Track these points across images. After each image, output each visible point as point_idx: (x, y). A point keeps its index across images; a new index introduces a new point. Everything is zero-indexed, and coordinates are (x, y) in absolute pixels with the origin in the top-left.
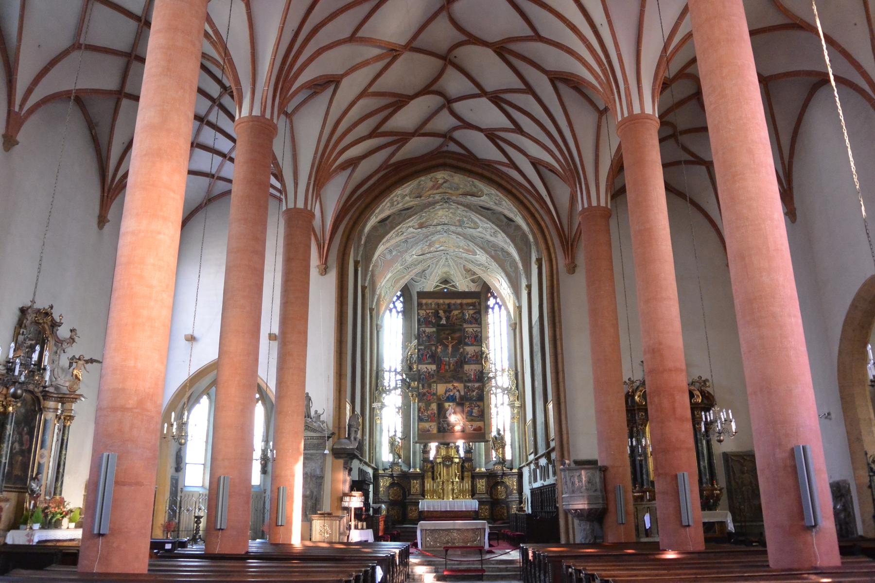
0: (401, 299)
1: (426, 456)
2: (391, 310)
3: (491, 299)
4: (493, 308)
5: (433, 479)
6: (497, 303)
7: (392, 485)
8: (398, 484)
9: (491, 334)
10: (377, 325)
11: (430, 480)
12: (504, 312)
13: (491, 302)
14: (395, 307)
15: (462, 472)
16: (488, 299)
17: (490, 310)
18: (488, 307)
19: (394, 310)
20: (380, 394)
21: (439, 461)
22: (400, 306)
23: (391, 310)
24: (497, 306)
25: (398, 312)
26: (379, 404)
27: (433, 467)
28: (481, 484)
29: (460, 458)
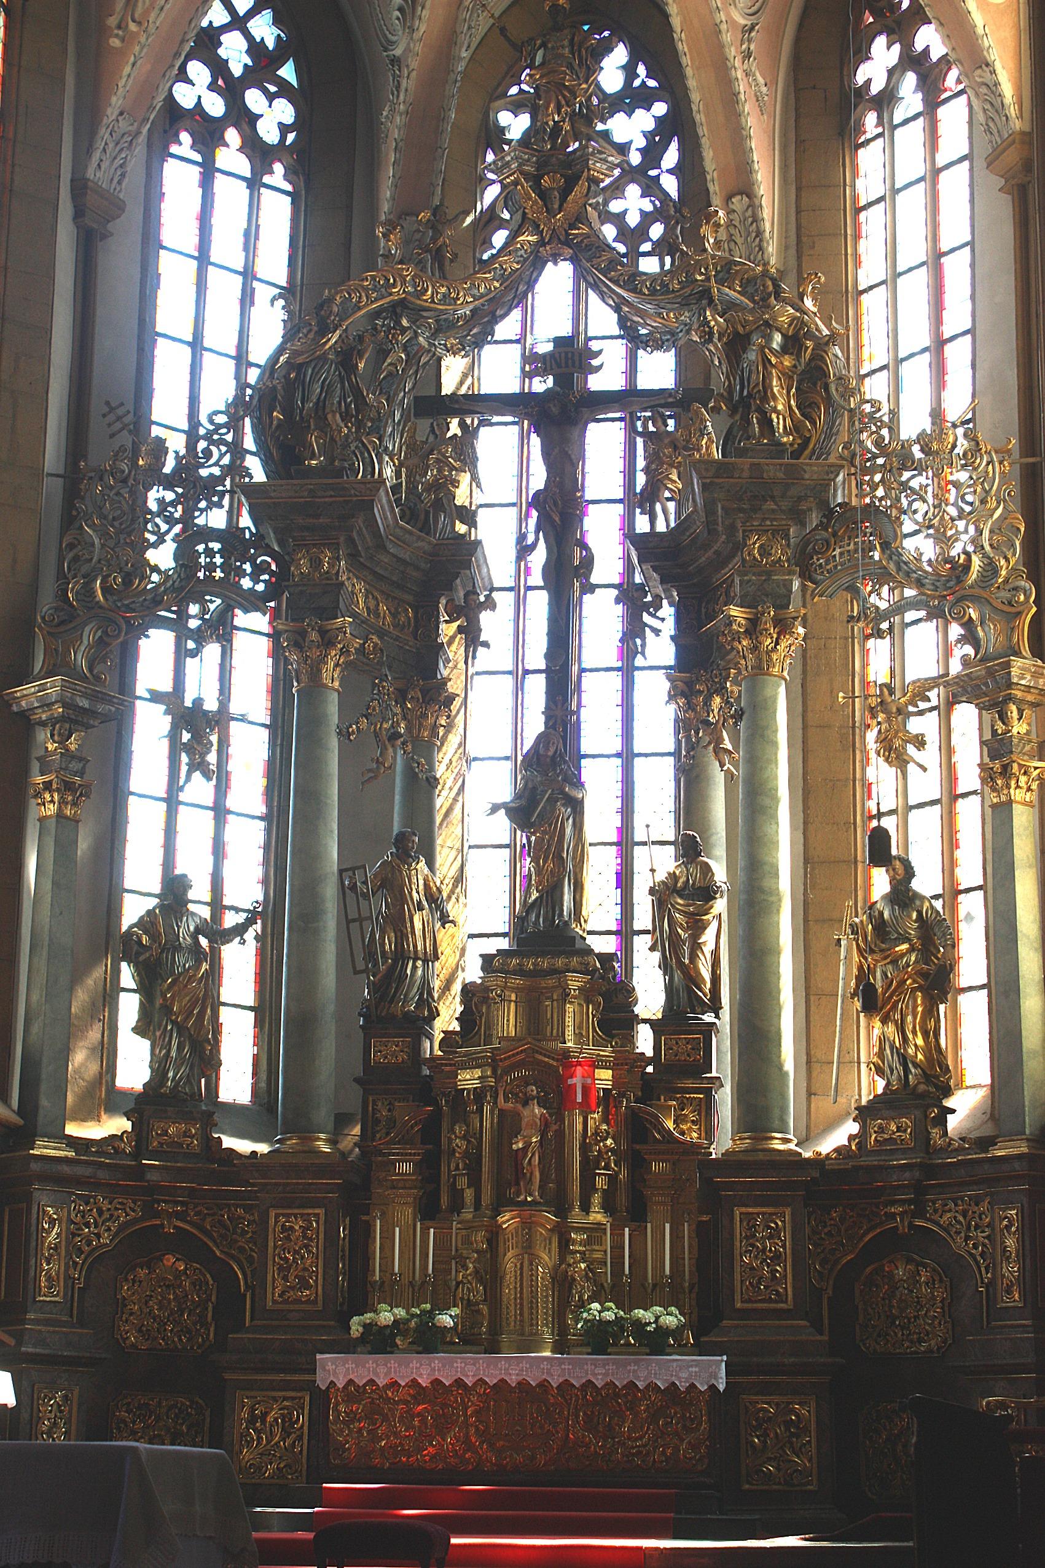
0: (288, 72)
1: (389, 1051)
2: (209, 136)
3: (881, 41)
4: (886, 100)
5: (429, 1211)
6: (913, 60)
7: (140, 1246)
8: (183, 1244)
9: (871, 267)
10: (80, 187)
11: (406, 1213)
12: (954, 117)
13: (879, 62)
14: (246, 120)
15: (637, 1162)
16: (863, 55)
17: (871, 119)
18: (855, 99)
19: (232, 136)
20: (66, 621)
21: (469, 1079)
22: (274, 116)
23: (209, 136)
24: (910, 79)
25: (260, 154)
26: (53, 686)
27: (431, 1132)
28: (768, 1248)
29: (627, 1062)
